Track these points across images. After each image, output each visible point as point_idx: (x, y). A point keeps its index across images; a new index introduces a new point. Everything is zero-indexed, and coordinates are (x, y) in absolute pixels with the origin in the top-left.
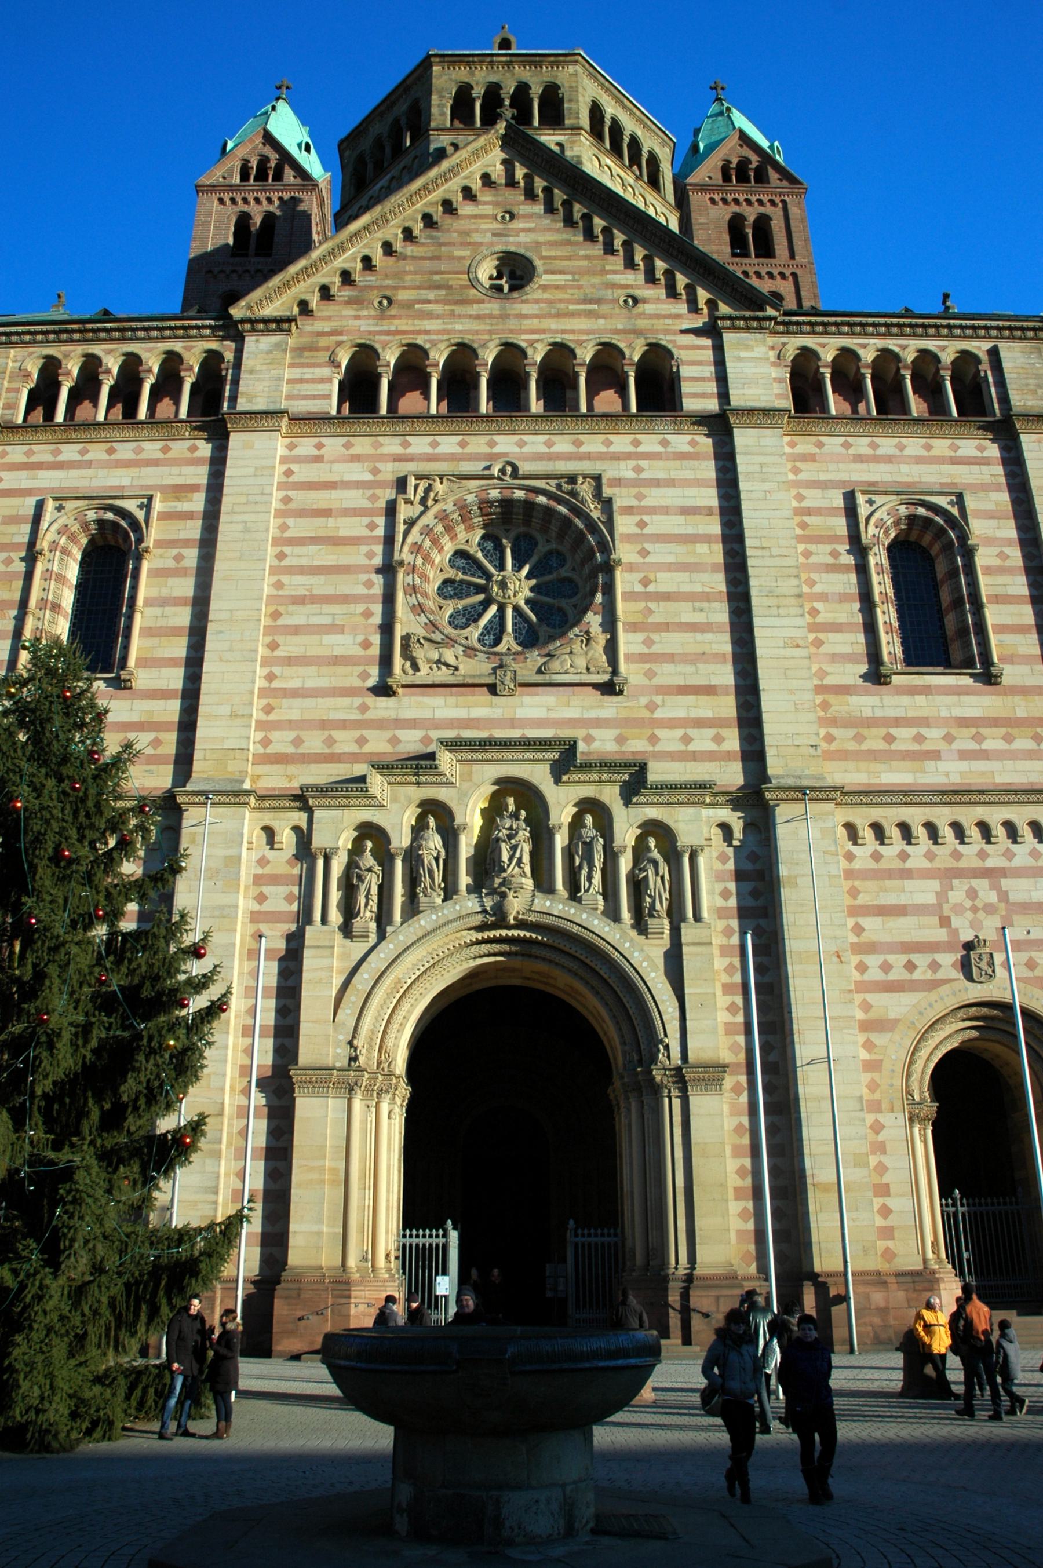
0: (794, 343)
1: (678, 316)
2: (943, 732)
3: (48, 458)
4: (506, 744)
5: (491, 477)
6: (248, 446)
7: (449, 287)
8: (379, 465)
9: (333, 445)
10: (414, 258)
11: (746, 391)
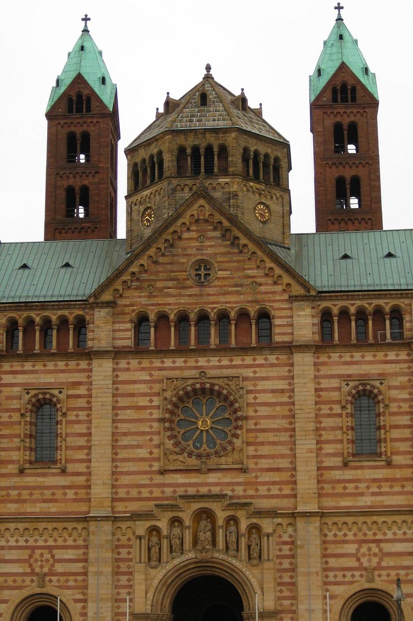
0: (325, 304)
1: (274, 293)
2: (366, 485)
3: (19, 368)
4: (203, 496)
5: (197, 378)
6: (100, 366)
7: (178, 280)
8: (153, 372)
9: (134, 363)
10: (163, 263)
11: (301, 333)
